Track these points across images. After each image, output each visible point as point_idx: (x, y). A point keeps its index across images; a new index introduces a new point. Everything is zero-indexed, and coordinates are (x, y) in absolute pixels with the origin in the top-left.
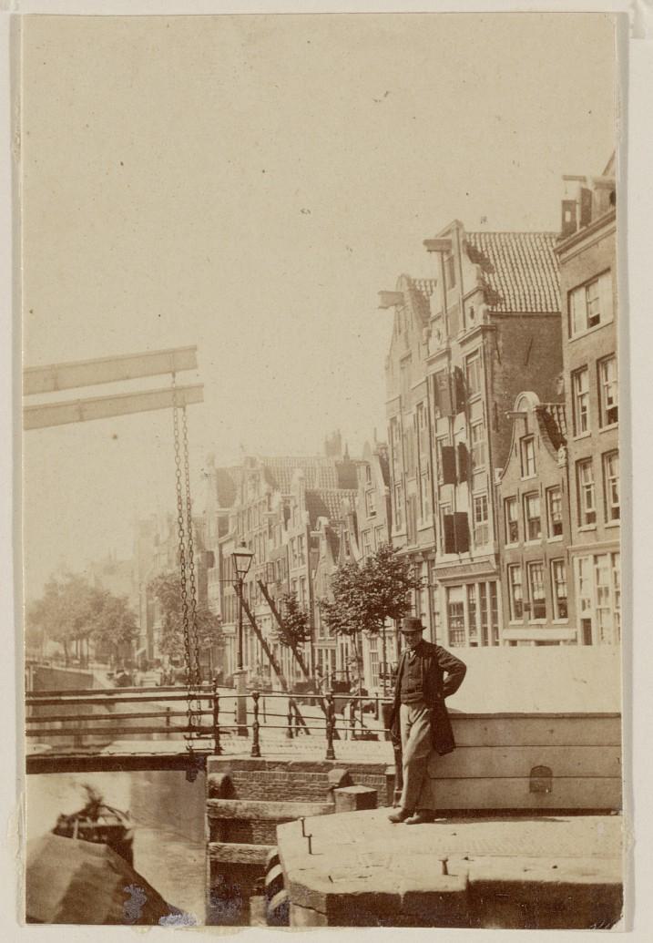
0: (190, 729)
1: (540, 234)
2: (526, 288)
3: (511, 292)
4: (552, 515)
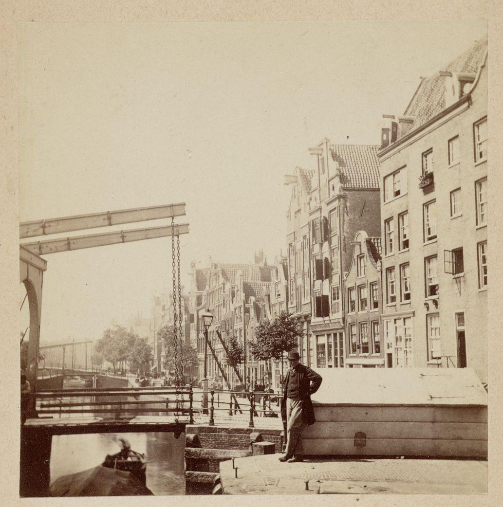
0: (177, 410)
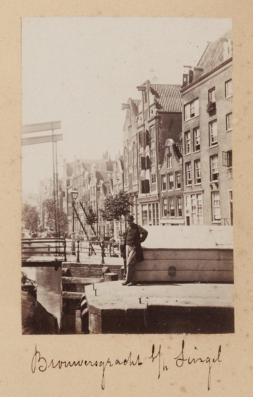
0: (56, 252)
1: (175, 85)
2: (170, 103)
3: (165, 105)
4: (177, 181)
